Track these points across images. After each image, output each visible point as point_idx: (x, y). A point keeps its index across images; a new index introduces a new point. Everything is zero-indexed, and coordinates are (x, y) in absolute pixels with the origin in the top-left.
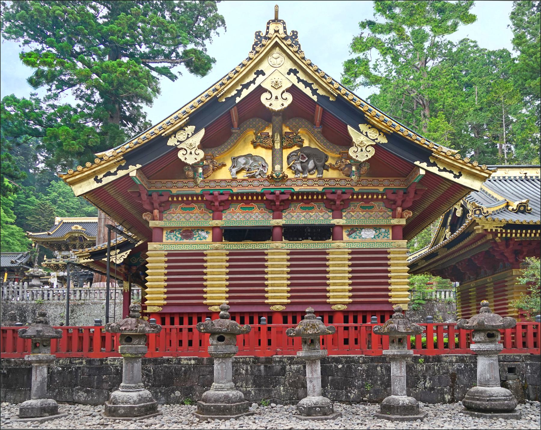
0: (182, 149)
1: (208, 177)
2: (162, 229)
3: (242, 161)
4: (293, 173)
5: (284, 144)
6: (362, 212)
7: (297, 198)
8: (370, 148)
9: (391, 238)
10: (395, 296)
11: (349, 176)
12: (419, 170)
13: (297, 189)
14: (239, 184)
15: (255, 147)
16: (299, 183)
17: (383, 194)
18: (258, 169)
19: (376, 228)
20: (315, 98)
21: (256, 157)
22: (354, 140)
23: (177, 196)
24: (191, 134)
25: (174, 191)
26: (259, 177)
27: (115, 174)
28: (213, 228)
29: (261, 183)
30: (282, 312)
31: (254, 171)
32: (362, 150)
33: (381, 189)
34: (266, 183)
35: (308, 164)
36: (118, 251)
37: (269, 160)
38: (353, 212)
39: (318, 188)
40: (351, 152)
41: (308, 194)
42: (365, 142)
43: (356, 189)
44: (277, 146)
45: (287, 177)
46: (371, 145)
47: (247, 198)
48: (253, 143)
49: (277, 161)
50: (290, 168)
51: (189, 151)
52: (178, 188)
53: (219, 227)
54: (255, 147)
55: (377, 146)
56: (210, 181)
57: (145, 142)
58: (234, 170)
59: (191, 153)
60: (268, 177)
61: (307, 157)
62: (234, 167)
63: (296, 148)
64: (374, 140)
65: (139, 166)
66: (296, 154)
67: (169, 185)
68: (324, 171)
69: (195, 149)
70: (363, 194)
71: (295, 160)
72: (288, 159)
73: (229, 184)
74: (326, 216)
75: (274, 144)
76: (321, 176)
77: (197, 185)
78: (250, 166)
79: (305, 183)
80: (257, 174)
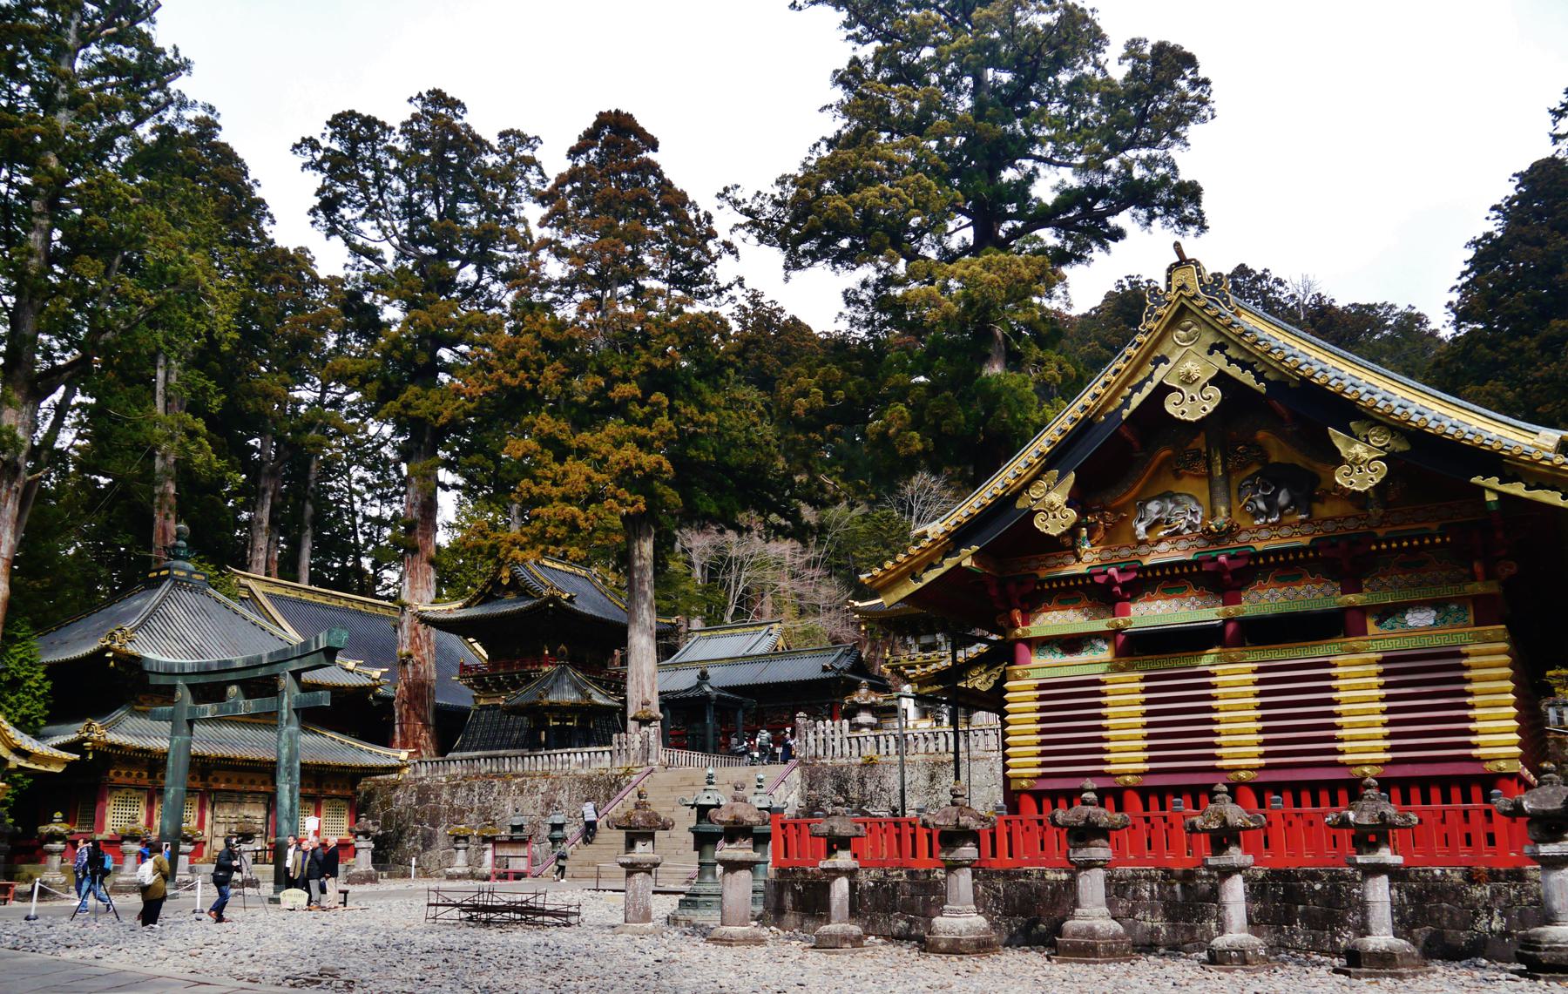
6: (1404, 574)
9: (1472, 622)
12: (1484, 495)
13: (1260, 547)
16: (1264, 534)
22: (1343, 455)
23: (1050, 581)
26: (1188, 531)
27: (941, 565)
33: (1434, 527)
34: (1200, 543)
38: (1384, 576)
39: (1301, 539)
41: (1285, 551)
45: (1238, 526)
64: (1382, 448)
65: (975, 548)
67: (1034, 564)
74: (1328, 589)
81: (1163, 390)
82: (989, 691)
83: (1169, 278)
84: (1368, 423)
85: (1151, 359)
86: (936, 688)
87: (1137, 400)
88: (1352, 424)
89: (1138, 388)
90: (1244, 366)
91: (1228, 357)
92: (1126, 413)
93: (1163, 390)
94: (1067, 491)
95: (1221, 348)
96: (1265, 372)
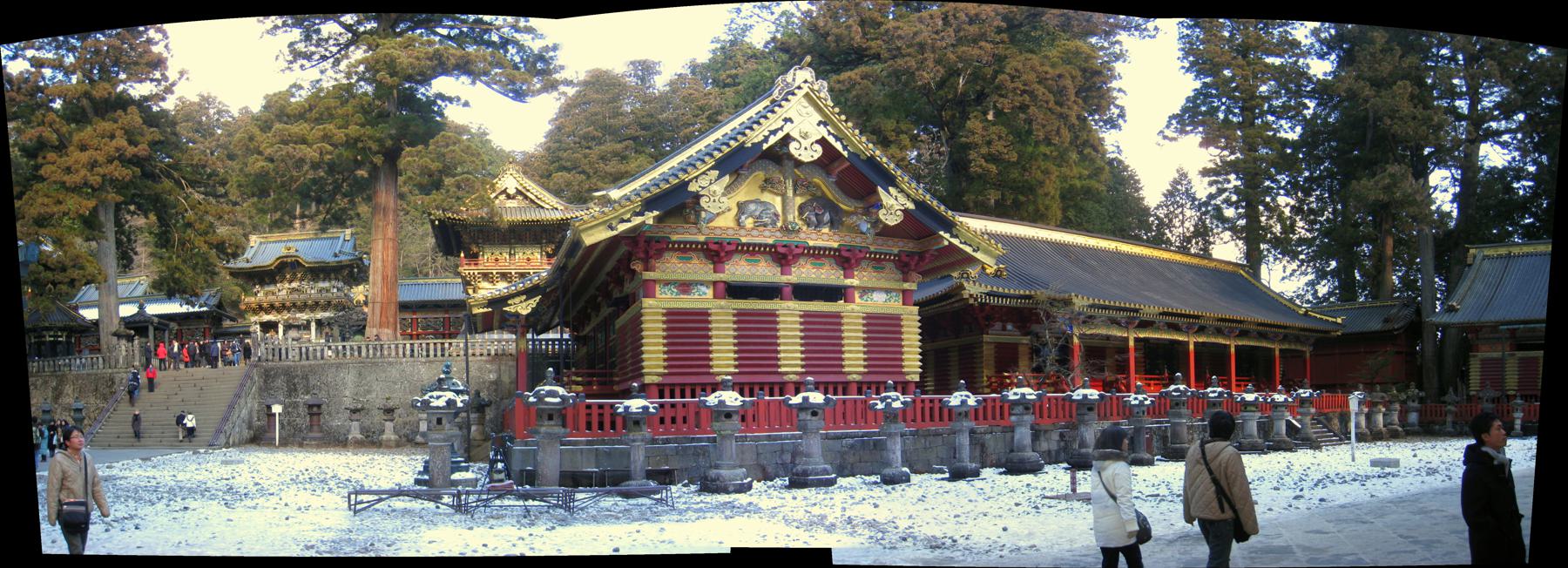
2: (654, 281)
7: (809, 251)
8: (899, 213)
10: (786, 366)
13: (811, 243)
17: (895, 256)
19: (887, 291)
20: (845, 154)
23: (675, 242)
25: (675, 238)
28: (715, 283)
30: (658, 385)
33: (896, 251)
34: (778, 234)
36: (524, 297)
40: (882, 214)
41: (820, 248)
43: (872, 249)
47: (754, 248)
51: (712, 199)
53: (725, 282)
55: (906, 211)
59: (714, 201)
60: (782, 227)
65: (656, 213)
70: (876, 253)
77: (700, 231)
81: (787, 139)
82: (528, 315)
86: (486, 310)
87: (773, 140)
89: (774, 132)
92: (765, 146)
93: (787, 139)
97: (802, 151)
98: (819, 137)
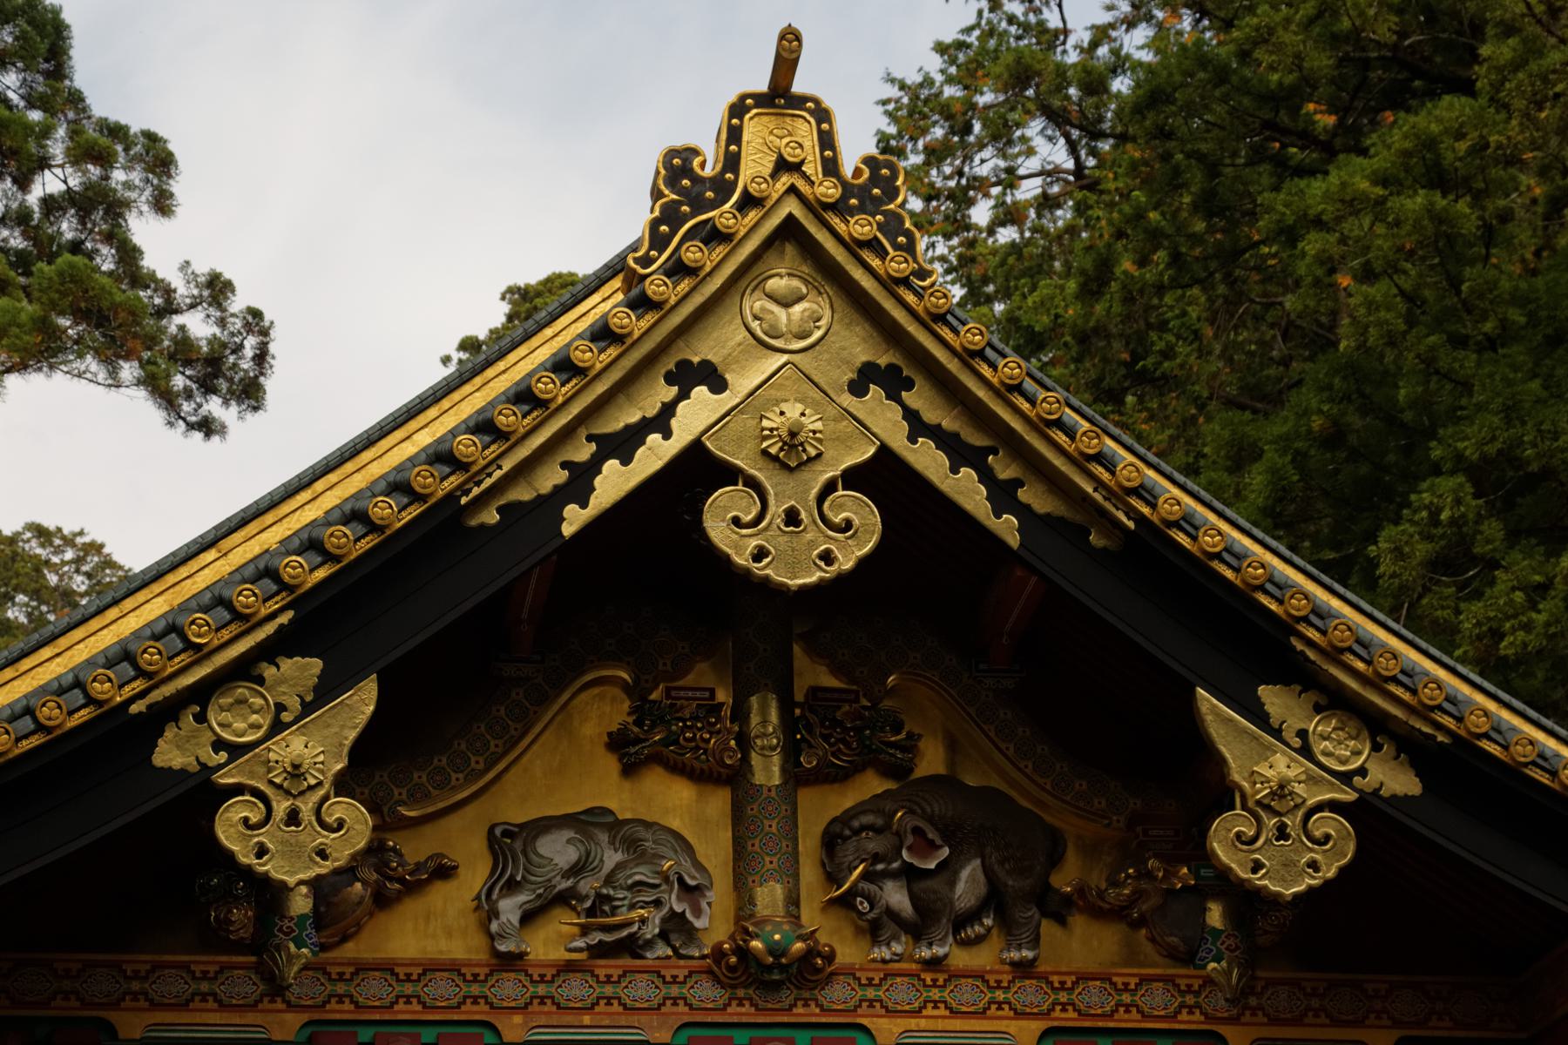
0: (238, 789)
1: (345, 939)
3: (558, 850)
4: (859, 931)
5: (808, 762)
8: (1327, 824)
11: (1188, 957)
14: (541, 990)
15: (630, 770)
16: (901, 993)
18: (657, 903)
21: (642, 832)
24: (294, 704)
26: (663, 950)
29: (675, 991)
31: (635, 914)
32: (1282, 833)
34: (706, 992)
35: (952, 883)
37: (715, 851)
42: (1299, 789)
44: (768, 771)
45: (830, 958)
46: (1333, 806)
48: (618, 743)
49: (770, 862)
50: (845, 902)
51: (281, 807)
52: (155, 1006)
54: (630, 770)
56: (361, 968)
57: (26, 745)
58: (510, 908)
59: (293, 818)
60: (718, 954)
61: (947, 840)
62: (512, 886)
63: (872, 785)
64: (1346, 778)
66: (880, 822)
68: (1048, 928)
69: (322, 792)
71: (877, 858)
72: (831, 841)
73: (475, 989)
75: (745, 759)
76: (1027, 954)
78: (609, 880)
79: (935, 994)
80: (651, 930)
83: (735, 135)
84: (1312, 697)
85: (670, 364)
88: (1262, 690)
89: (624, 445)
90: (959, 453)
91: (911, 415)
92: (574, 519)
94: (352, 735)
95: (894, 383)
96: (1018, 483)
97: (773, 535)
98: (872, 451)
